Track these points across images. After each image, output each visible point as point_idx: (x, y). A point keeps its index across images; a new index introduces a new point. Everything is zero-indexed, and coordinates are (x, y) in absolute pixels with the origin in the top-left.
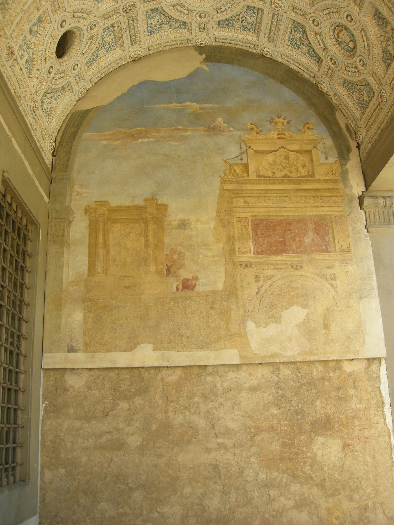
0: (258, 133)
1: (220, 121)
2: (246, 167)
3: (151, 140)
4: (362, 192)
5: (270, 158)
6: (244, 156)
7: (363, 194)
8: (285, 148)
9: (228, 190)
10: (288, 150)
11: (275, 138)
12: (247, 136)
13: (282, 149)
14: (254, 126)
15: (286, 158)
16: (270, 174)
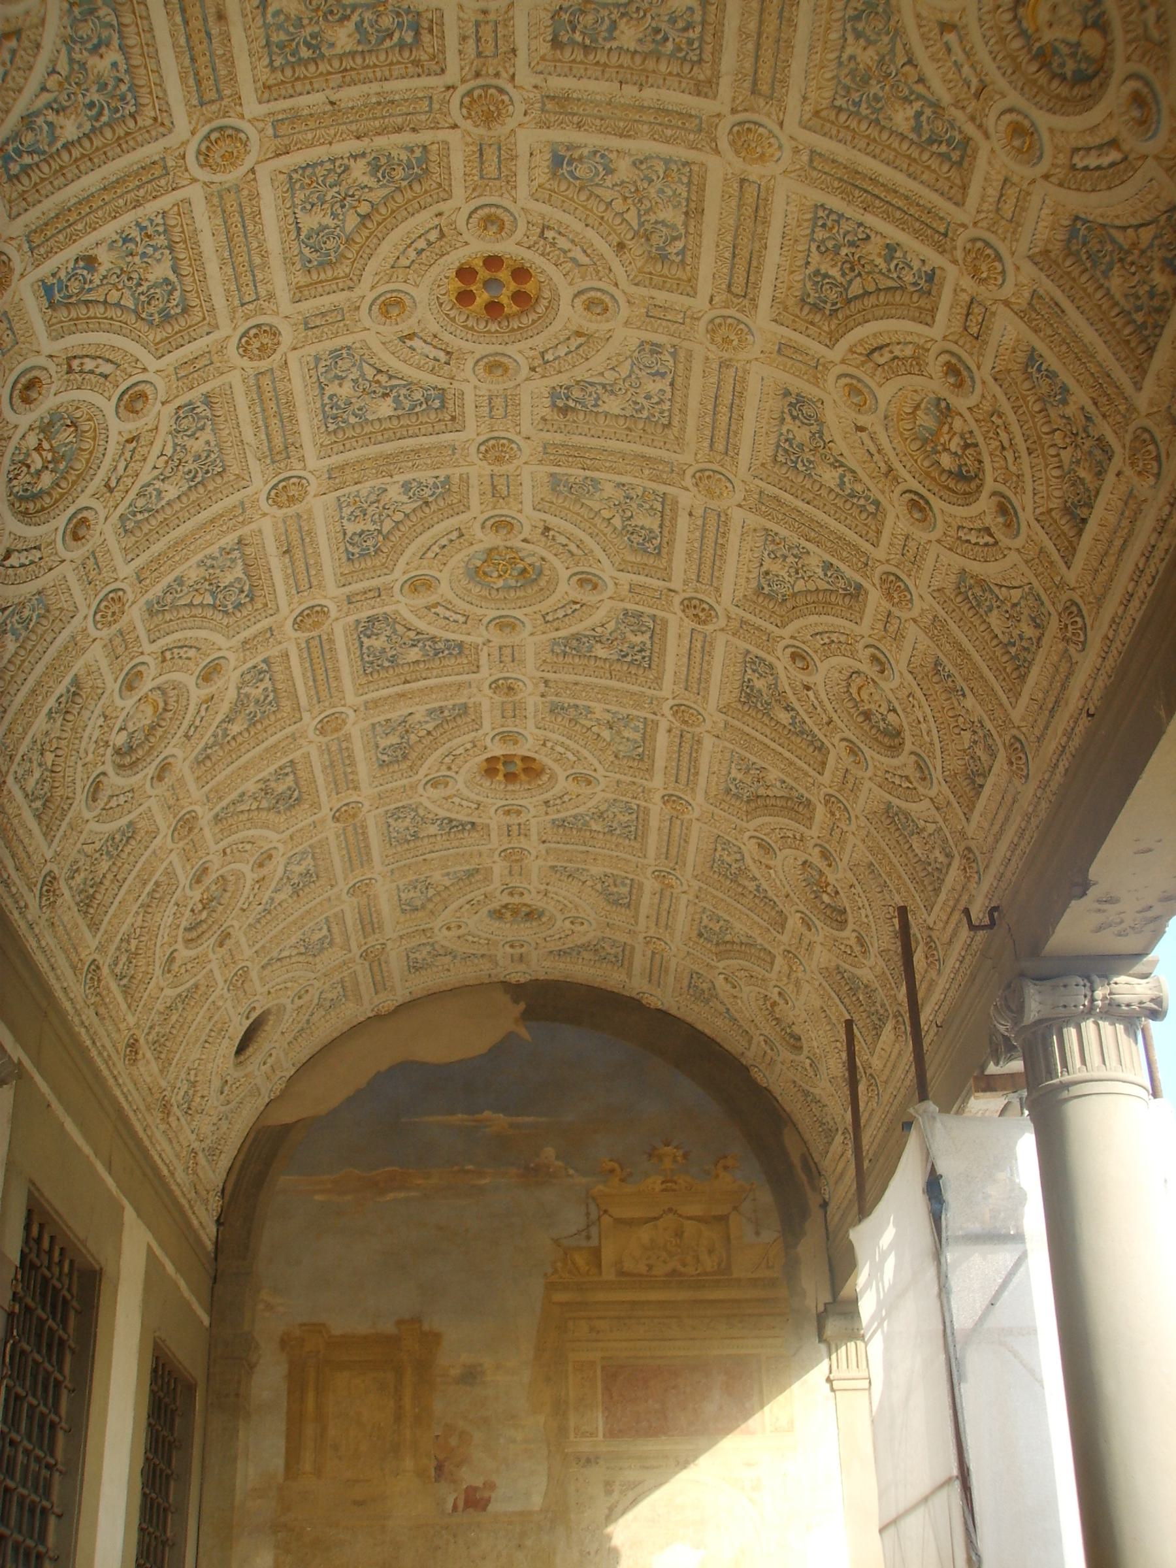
0: (622, 1180)
1: (549, 1152)
2: (596, 1253)
3: (412, 1194)
4: (825, 1304)
5: (645, 1234)
6: (594, 1231)
7: (825, 1310)
8: (676, 1212)
9: (561, 1304)
10: (680, 1216)
11: (657, 1190)
12: (601, 1187)
13: (671, 1215)
14: (616, 1166)
15: (676, 1235)
16: (643, 1269)
